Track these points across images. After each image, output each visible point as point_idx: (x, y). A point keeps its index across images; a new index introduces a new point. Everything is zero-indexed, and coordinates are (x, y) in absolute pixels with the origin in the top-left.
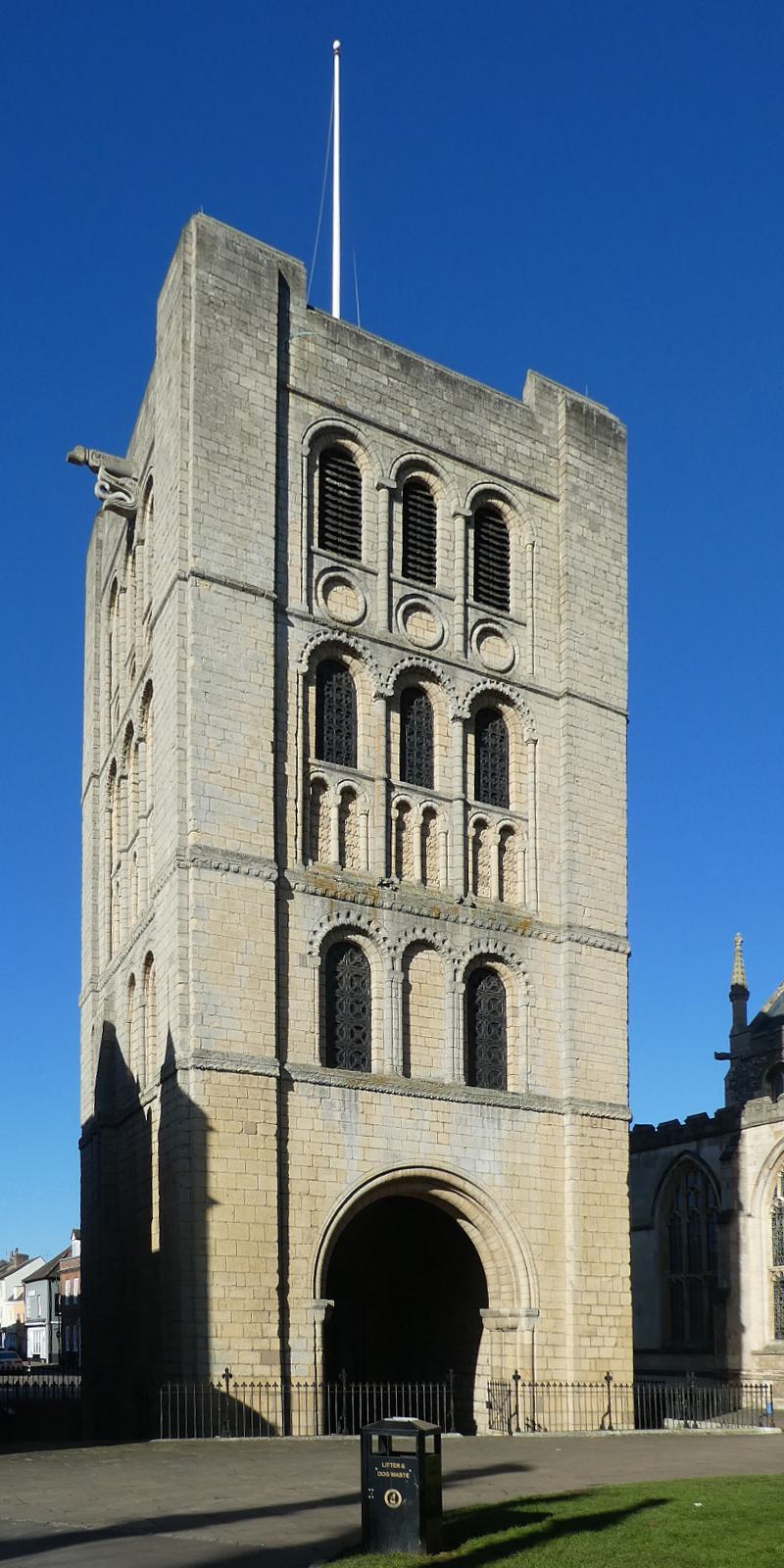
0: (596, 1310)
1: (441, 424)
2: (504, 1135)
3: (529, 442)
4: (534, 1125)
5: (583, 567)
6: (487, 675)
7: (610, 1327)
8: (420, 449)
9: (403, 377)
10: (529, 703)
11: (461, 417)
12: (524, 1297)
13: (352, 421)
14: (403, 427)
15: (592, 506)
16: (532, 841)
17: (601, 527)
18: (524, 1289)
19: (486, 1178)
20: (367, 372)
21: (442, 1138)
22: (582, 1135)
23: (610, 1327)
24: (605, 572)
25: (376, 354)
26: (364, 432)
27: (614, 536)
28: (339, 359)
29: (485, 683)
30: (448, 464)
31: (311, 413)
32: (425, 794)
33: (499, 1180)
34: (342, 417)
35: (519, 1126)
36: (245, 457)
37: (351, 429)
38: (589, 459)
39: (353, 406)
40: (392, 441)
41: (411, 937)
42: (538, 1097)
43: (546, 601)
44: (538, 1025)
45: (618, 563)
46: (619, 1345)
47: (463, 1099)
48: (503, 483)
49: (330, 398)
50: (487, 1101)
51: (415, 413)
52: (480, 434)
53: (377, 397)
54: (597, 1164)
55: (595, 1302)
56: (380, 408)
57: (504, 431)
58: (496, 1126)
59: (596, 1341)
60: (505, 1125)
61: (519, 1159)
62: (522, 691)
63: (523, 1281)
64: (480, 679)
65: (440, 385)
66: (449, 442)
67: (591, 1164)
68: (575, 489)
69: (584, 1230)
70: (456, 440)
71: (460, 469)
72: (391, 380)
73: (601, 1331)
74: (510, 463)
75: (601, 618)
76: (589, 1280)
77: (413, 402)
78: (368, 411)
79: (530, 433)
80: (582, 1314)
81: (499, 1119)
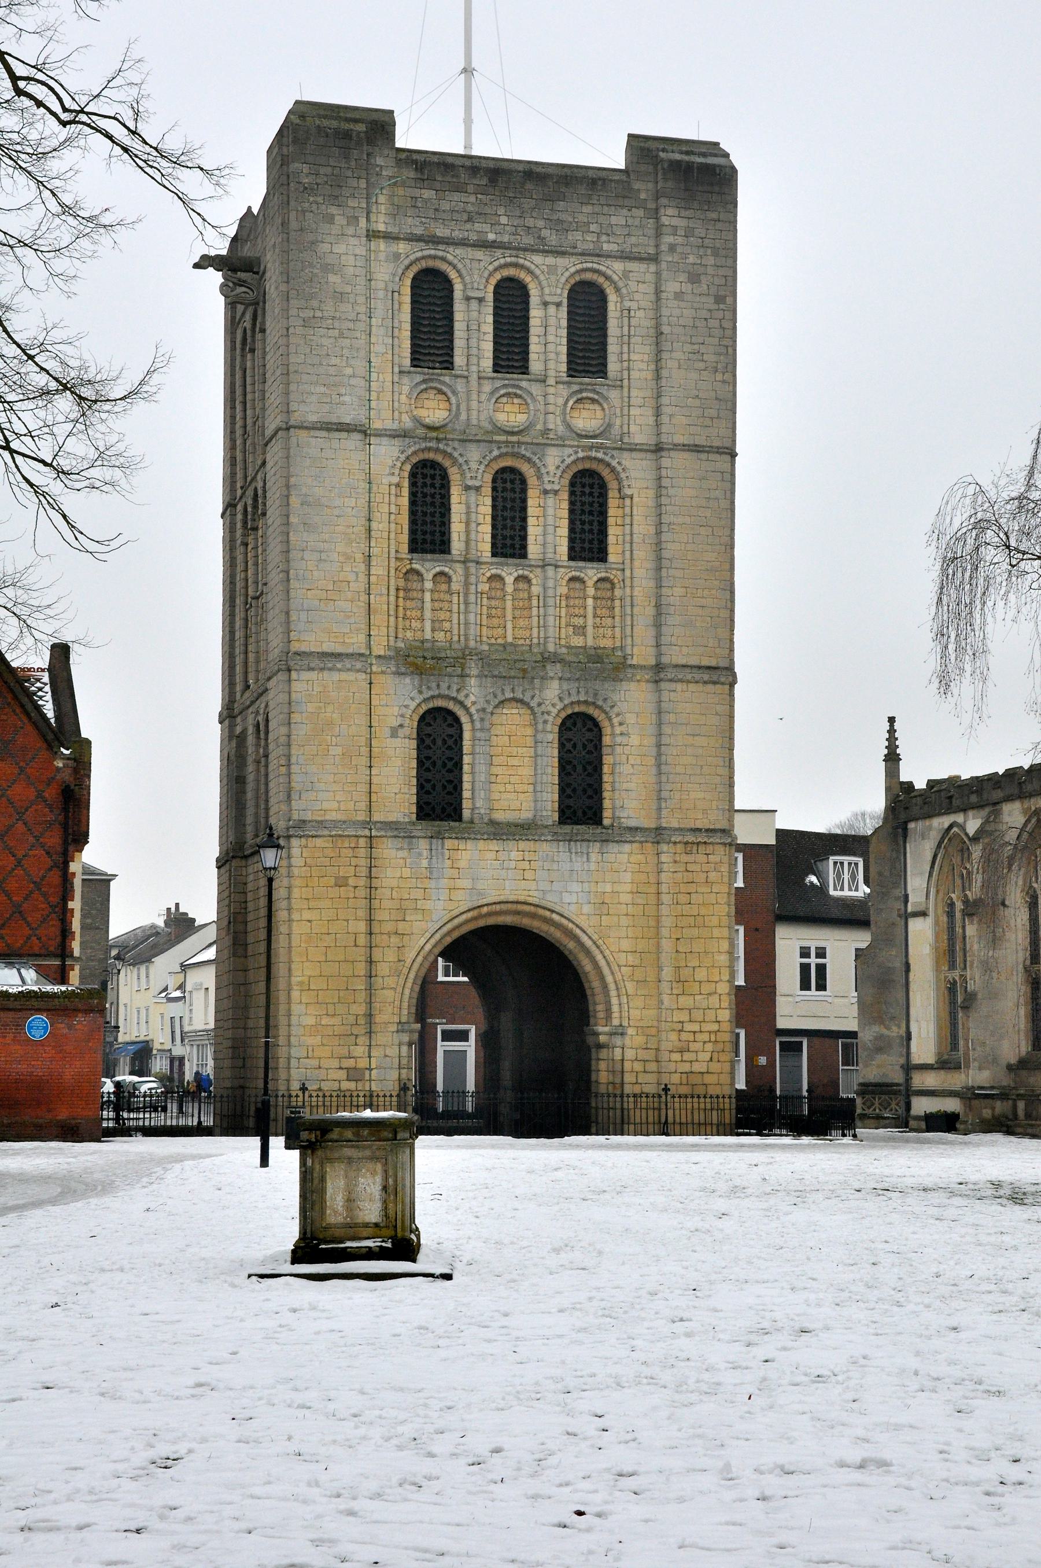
0: (688, 1027)
1: (530, 222)
2: (593, 866)
3: (625, 212)
4: (626, 856)
5: (682, 322)
6: (578, 447)
7: (705, 1042)
8: (508, 252)
9: (491, 190)
10: (624, 462)
11: (551, 210)
12: (616, 1015)
13: (440, 247)
14: (491, 237)
15: (691, 259)
16: (628, 590)
17: (702, 277)
18: (615, 1008)
19: (573, 908)
20: (456, 196)
21: (528, 875)
22: (675, 862)
23: (705, 1042)
24: (706, 319)
25: (463, 176)
26: (453, 254)
27: (717, 281)
28: (428, 194)
29: (576, 452)
30: (538, 259)
31: (401, 251)
32: (517, 565)
33: (587, 909)
34: (431, 246)
35: (610, 857)
36: (338, 315)
37: (440, 254)
38: (688, 213)
39: (441, 232)
40: (479, 254)
41: (501, 698)
42: (630, 829)
43: (642, 361)
44: (632, 761)
45: (722, 306)
46: (715, 1058)
47: (549, 838)
48: (595, 259)
49: (419, 231)
50: (575, 838)
51: (504, 220)
52: (571, 220)
53: (465, 217)
54: (692, 888)
55: (687, 1018)
56: (468, 226)
57: (597, 209)
58: (585, 859)
59: (687, 1056)
60: (594, 857)
61: (608, 888)
62: (615, 453)
63: (614, 1001)
64: (570, 451)
65: (529, 186)
66: (539, 237)
67: (683, 888)
68: (672, 248)
69: (677, 951)
70: (545, 233)
71: (550, 260)
72: (479, 196)
73: (693, 1046)
74: (604, 238)
75: (701, 365)
76: (681, 999)
77: (501, 211)
78: (457, 232)
79: (627, 202)
80: (674, 1030)
81: (588, 854)
